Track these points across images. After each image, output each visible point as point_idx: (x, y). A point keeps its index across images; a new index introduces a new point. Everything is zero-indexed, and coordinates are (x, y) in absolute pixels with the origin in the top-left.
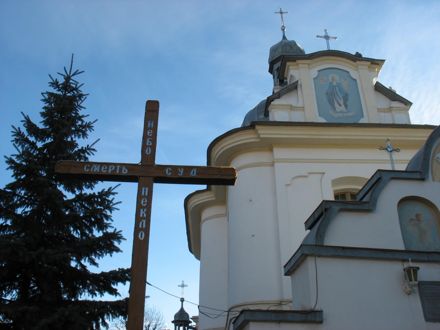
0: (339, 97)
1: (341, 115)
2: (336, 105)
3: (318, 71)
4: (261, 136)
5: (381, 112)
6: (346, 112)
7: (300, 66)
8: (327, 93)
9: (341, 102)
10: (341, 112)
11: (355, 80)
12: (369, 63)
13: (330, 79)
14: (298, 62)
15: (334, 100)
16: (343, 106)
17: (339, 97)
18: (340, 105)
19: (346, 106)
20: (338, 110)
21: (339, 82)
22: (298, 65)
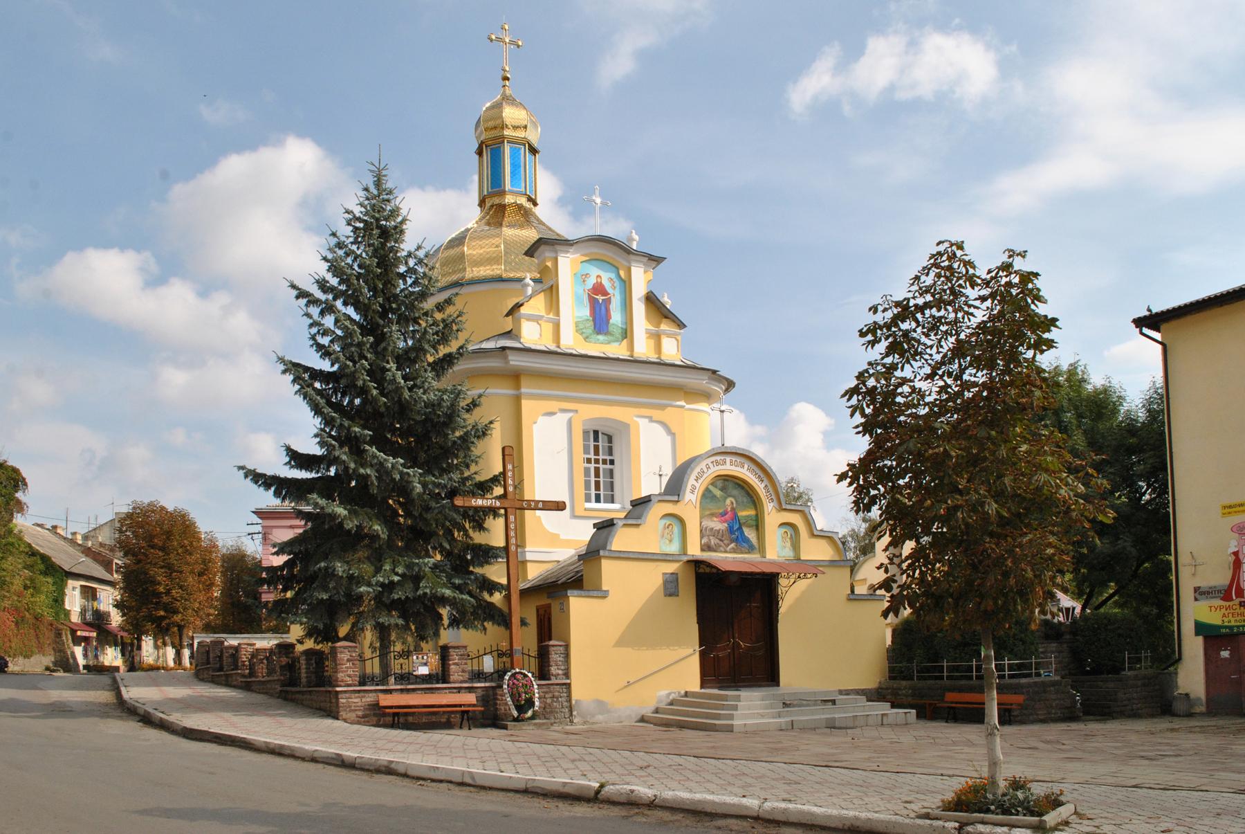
12: (645, 259)
22: (556, 252)
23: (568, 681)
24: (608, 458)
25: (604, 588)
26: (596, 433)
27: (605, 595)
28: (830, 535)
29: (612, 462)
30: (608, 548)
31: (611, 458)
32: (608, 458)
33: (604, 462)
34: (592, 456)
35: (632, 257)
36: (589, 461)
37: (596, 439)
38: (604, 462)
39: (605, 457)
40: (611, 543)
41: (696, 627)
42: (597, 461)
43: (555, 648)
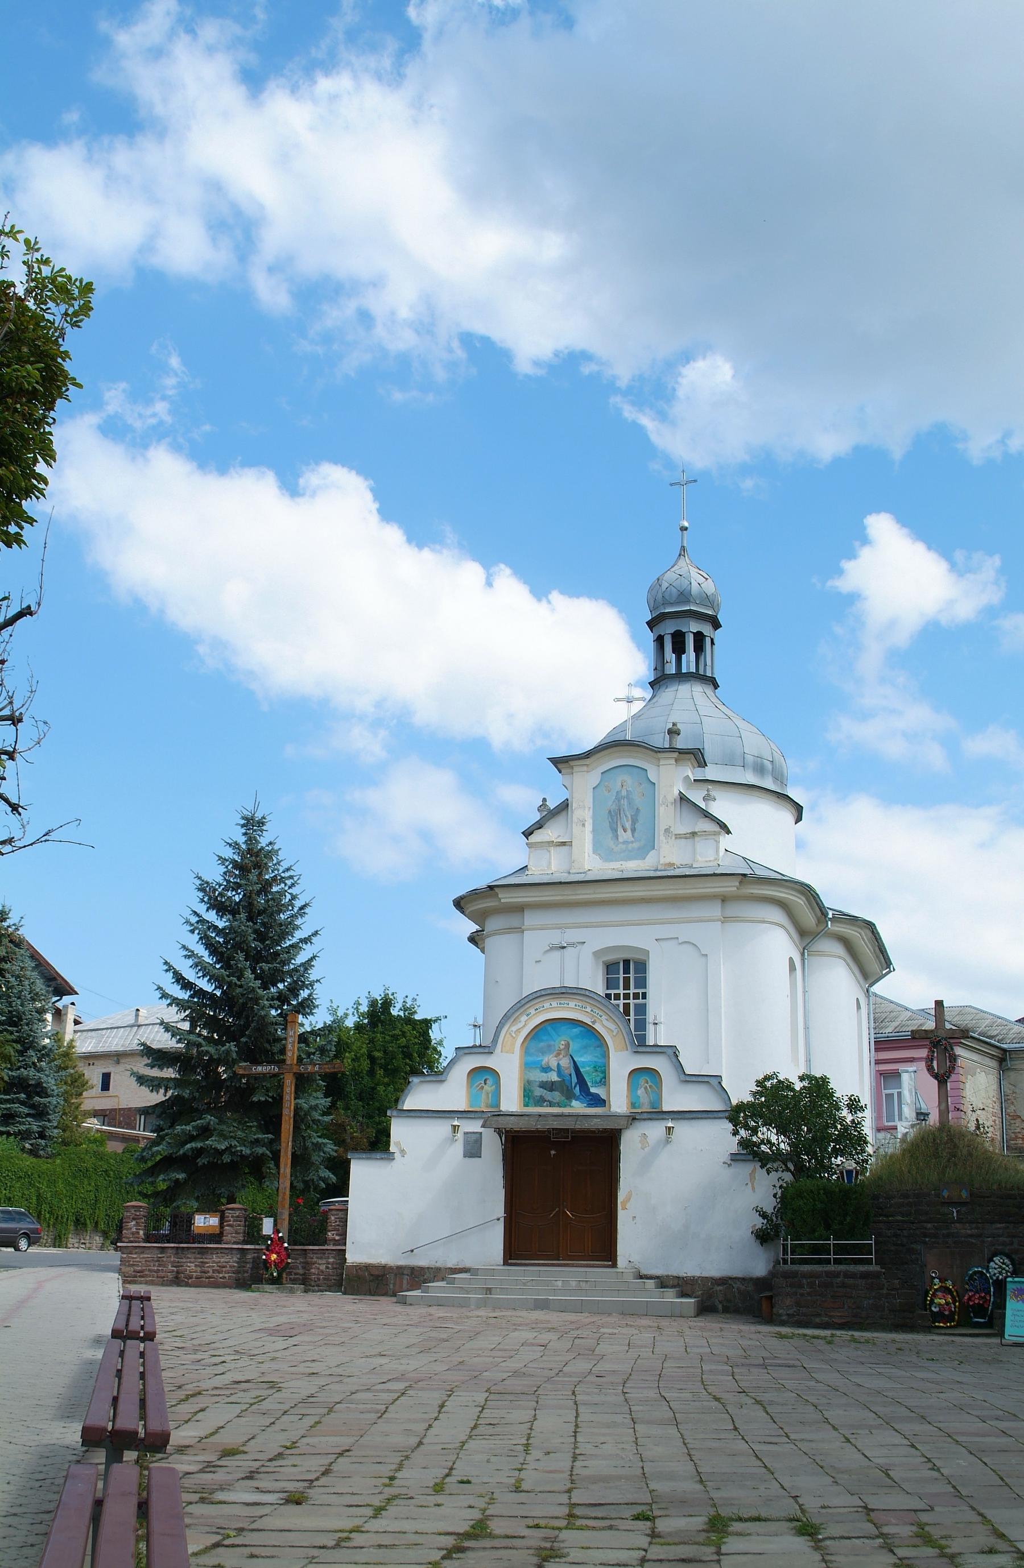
1: (624, 847)
2: (620, 831)
3: (602, 773)
5: (680, 838)
6: (632, 842)
8: (610, 812)
9: (628, 825)
10: (625, 842)
11: (654, 784)
12: (676, 755)
14: (572, 763)
15: (619, 824)
16: (629, 832)
18: (625, 831)
19: (633, 830)
20: (621, 840)
21: (630, 789)
23: (343, 1248)
24: (640, 991)
25: (392, 1149)
26: (627, 962)
28: (706, 1079)
30: (399, 1107)
31: (643, 991)
32: (640, 991)
33: (636, 996)
34: (621, 991)
36: (617, 997)
37: (627, 970)
38: (636, 996)
39: (637, 991)
40: (403, 1103)
42: (627, 996)
43: (334, 1212)
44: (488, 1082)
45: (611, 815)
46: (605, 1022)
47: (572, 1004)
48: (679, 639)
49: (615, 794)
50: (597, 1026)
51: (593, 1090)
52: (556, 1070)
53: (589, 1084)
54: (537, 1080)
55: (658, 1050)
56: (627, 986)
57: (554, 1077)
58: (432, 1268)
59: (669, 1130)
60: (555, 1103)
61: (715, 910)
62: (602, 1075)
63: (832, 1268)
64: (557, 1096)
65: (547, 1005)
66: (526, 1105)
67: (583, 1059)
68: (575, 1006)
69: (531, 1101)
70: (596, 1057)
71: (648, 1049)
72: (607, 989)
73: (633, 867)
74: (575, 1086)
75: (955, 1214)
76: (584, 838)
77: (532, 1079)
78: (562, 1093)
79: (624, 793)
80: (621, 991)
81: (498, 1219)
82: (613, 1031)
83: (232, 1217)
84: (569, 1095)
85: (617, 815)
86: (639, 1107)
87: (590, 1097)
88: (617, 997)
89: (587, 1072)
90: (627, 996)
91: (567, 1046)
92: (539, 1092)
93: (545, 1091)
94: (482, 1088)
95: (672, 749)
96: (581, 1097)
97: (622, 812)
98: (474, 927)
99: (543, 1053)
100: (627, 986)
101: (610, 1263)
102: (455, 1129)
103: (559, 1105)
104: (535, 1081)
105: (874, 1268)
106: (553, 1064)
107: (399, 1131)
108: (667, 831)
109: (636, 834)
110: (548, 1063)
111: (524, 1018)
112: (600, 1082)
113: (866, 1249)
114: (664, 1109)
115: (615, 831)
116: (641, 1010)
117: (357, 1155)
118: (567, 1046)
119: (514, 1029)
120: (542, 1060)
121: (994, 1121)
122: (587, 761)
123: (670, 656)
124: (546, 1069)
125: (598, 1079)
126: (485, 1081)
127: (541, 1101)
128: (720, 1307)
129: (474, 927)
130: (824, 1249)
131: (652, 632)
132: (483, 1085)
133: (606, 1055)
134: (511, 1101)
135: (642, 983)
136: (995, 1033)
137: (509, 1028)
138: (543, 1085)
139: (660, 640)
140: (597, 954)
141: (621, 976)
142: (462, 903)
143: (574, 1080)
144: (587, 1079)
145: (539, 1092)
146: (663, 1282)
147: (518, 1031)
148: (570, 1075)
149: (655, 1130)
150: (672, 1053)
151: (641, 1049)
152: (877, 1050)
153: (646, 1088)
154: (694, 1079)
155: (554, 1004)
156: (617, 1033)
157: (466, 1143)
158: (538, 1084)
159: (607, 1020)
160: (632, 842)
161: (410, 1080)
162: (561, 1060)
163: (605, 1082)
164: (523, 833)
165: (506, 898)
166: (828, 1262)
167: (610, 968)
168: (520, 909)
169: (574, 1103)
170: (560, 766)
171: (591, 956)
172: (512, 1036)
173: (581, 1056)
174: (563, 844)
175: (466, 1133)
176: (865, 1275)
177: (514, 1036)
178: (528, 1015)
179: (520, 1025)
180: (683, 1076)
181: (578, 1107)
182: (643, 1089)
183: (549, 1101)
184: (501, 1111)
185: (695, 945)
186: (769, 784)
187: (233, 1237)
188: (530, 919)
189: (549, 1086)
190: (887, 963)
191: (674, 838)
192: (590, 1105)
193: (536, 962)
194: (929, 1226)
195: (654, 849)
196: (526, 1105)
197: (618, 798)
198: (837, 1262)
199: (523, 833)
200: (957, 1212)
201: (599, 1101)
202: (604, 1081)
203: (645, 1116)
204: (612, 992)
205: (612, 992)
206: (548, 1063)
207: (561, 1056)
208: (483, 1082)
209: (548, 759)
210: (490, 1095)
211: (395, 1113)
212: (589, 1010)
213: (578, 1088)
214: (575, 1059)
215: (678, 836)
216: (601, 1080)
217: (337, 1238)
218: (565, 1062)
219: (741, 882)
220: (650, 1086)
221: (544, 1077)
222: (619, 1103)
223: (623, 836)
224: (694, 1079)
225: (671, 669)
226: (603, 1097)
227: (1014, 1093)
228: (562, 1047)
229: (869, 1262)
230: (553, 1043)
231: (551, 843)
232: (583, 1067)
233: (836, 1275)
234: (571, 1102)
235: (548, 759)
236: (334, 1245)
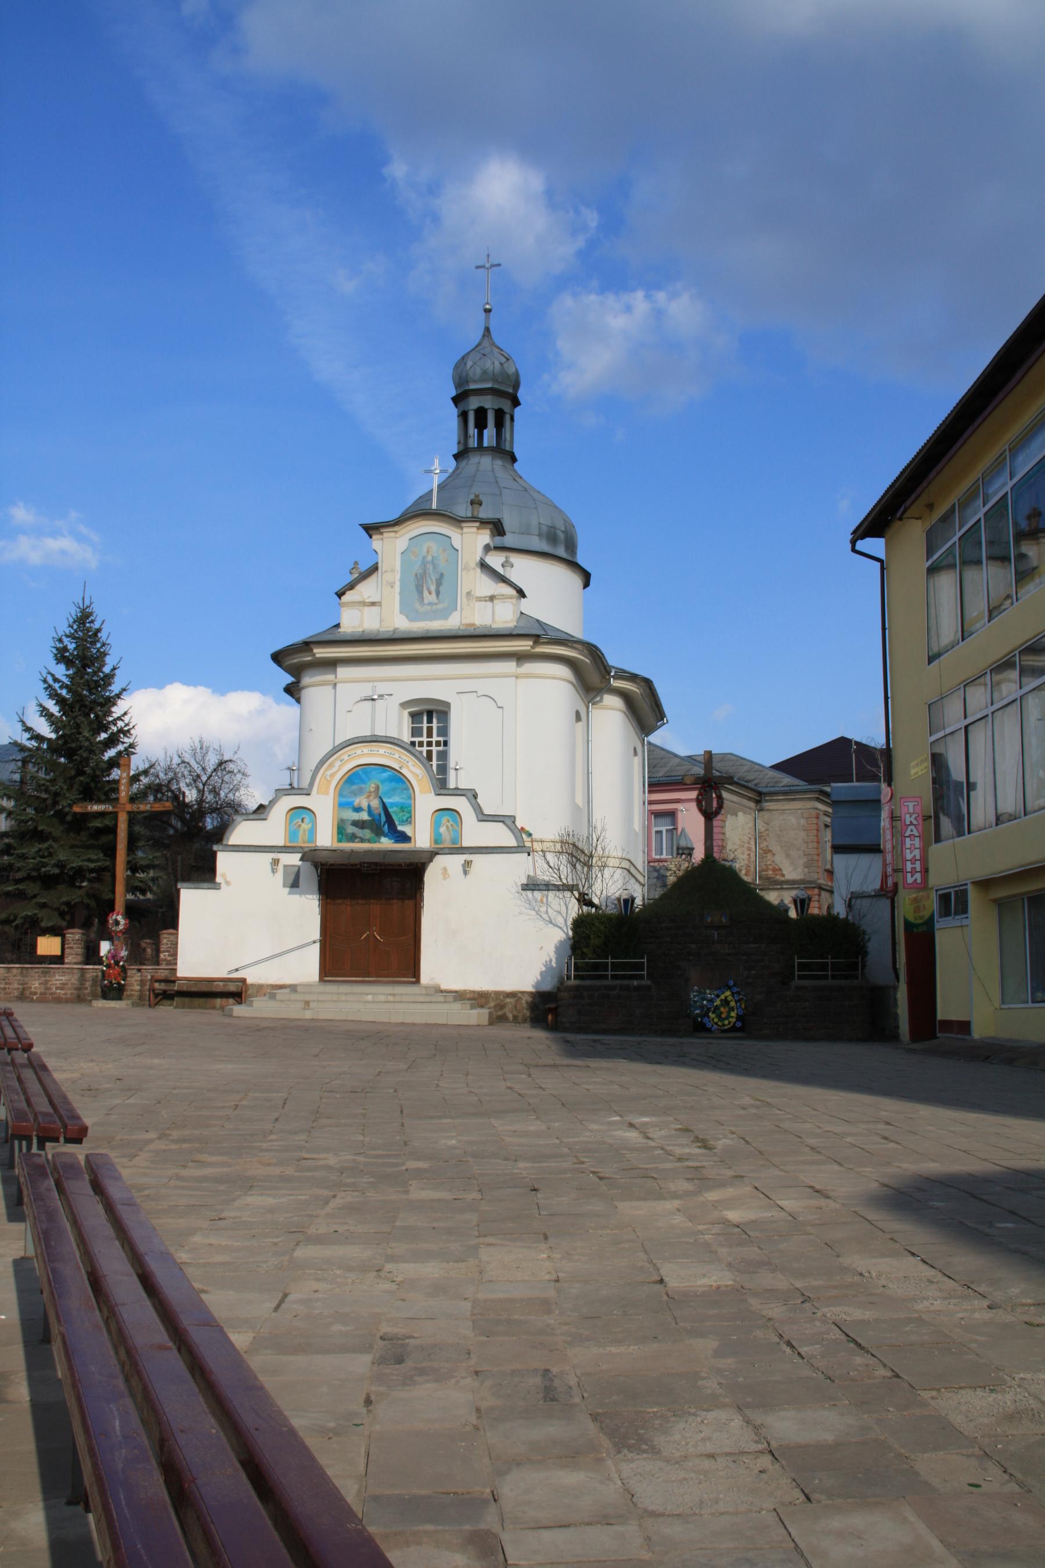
0: (431, 580)
1: (428, 608)
2: (426, 593)
3: (410, 539)
4: (317, 656)
5: (481, 601)
6: (436, 604)
7: (385, 535)
8: (416, 575)
9: (433, 588)
10: (430, 604)
11: (457, 550)
12: (477, 524)
13: (425, 550)
17: (431, 580)
18: (430, 593)
19: (438, 593)
20: (426, 601)
24: (441, 739)
25: (218, 879)
27: (217, 887)
28: (501, 819)
29: (446, 743)
30: (225, 842)
31: (445, 739)
32: (441, 739)
33: (438, 744)
34: (425, 739)
35: (464, 525)
36: (421, 744)
37: (430, 721)
38: (438, 744)
40: (228, 839)
41: (319, 918)
42: (430, 744)
44: (305, 820)
45: (418, 579)
46: (412, 768)
47: (382, 751)
48: (481, 414)
49: (421, 559)
50: (404, 771)
51: (400, 828)
52: (367, 809)
53: (397, 823)
54: (350, 819)
55: (458, 792)
56: (430, 735)
57: (364, 816)
58: (255, 985)
59: (468, 864)
60: (366, 840)
61: (509, 667)
62: (408, 815)
63: (609, 982)
64: (367, 833)
65: (359, 752)
66: (340, 841)
67: (391, 801)
68: (385, 752)
69: (344, 838)
70: (403, 798)
71: (450, 792)
72: (413, 736)
73: (436, 625)
74: (384, 825)
75: (716, 936)
76: (393, 600)
77: (345, 817)
78: (372, 831)
79: (429, 558)
80: (425, 739)
81: (314, 942)
82: (418, 776)
83: (73, 940)
84: (378, 832)
85: (423, 579)
86: (441, 843)
87: (398, 835)
88: (421, 744)
89: (395, 812)
90: (430, 744)
91: (377, 788)
92: (351, 829)
93: (357, 829)
94: (300, 826)
95: (474, 519)
96: (389, 834)
97: (427, 576)
98: (289, 679)
99: (355, 794)
100: (430, 735)
101: (414, 979)
102: (275, 862)
103: (369, 841)
104: (348, 820)
105: (646, 982)
106: (365, 805)
107: (224, 861)
108: (469, 594)
109: (440, 597)
110: (360, 804)
111: (338, 763)
112: (407, 821)
113: (639, 967)
114: (465, 844)
115: (420, 592)
116: (443, 756)
117: (185, 885)
118: (377, 788)
119: (329, 773)
120: (354, 801)
121: (749, 855)
122: (396, 528)
123: (473, 431)
124: (358, 809)
125: (405, 818)
126: (303, 820)
127: (353, 838)
128: (510, 1016)
129: (289, 679)
130: (605, 967)
131: (456, 406)
132: (300, 823)
133: (412, 797)
134: (325, 838)
135: (444, 731)
136: (752, 777)
137: (325, 772)
138: (357, 824)
139: (464, 416)
140: (404, 705)
141: (425, 725)
142: (280, 658)
143: (383, 819)
144: (395, 817)
145: (351, 829)
146: (460, 996)
147: (332, 775)
148: (380, 815)
149: (453, 862)
150: (472, 796)
151: (442, 792)
152: (650, 792)
153: (447, 827)
154: (490, 818)
155: (366, 751)
156: (422, 778)
157: (286, 875)
158: (350, 822)
159: (413, 765)
160: (436, 604)
161: (234, 818)
162: (371, 801)
163: (411, 821)
164: (336, 593)
165: (321, 652)
166: (605, 977)
167: (415, 716)
168: (332, 664)
169: (383, 839)
170: (371, 532)
171: (397, 705)
172: (327, 780)
173: (390, 797)
174: (373, 604)
175: (285, 866)
176: (637, 988)
177: (329, 778)
178: (341, 761)
179: (334, 770)
180: (481, 815)
181: (386, 843)
182: (444, 828)
183: (360, 838)
184: (316, 846)
185: (494, 700)
186: (561, 552)
187: (74, 957)
188: (343, 672)
189: (360, 824)
190: (660, 715)
191: (474, 600)
192: (397, 841)
193: (348, 711)
194: (694, 946)
195: (456, 609)
196: (340, 841)
197: (424, 563)
198: (614, 977)
199: (336, 593)
200: (718, 934)
201: (404, 838)
202: (409, 820)
203: (447, 851)
204: (417, 740)
205: (417, 740)
206: (360, 804)
207: (371, 798)
208: (300, 820)
209: (360, 525)
210: (307, 832)
211: (220, 847)
212: (397, 756)
213: (386, 826)
214: (385, 800)
215: (479, 599)
216: (408, 819)
217: (169, 958)
218: (375, 803)
219: (535, 643)
220: (452, 825)
221: (356, 816)
222: (422, 839)
223: (430, 598)
224: (490, 818)
225: (473, 443)
226: (409, 833)
227: (767, 830)
228: (372, 790)
229: (641, 977)
230: (364, 786)
231: (364, 604)
232: (392, 807)
233: (614, 988)
234: (380, 839)
235: (360, 525)
236: (167, 964)
